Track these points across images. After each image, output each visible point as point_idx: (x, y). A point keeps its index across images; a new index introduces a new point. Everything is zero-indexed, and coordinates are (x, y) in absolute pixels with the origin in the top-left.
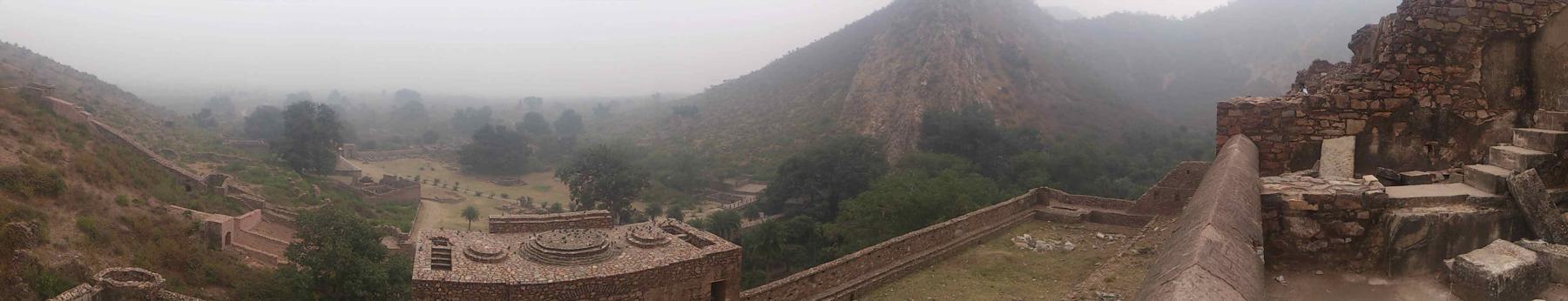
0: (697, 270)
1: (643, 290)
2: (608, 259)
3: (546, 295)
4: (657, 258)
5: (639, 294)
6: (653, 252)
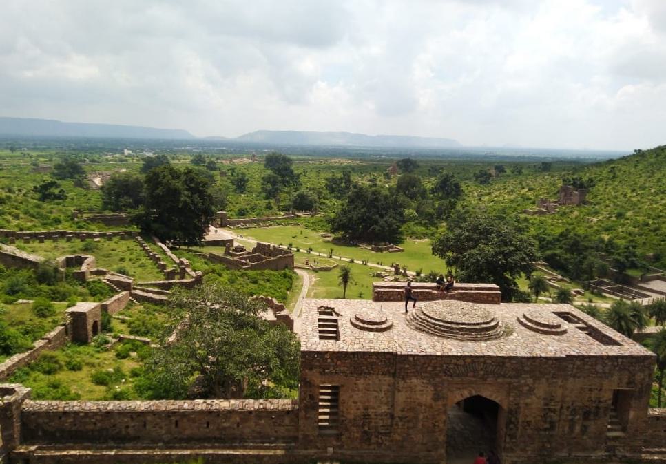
0: (599, 368)
1: (536, 379)
2: (497, 337)
3: (434, 368)
4: (550, 347)
5: (530, 381)
6: (547, 339)
